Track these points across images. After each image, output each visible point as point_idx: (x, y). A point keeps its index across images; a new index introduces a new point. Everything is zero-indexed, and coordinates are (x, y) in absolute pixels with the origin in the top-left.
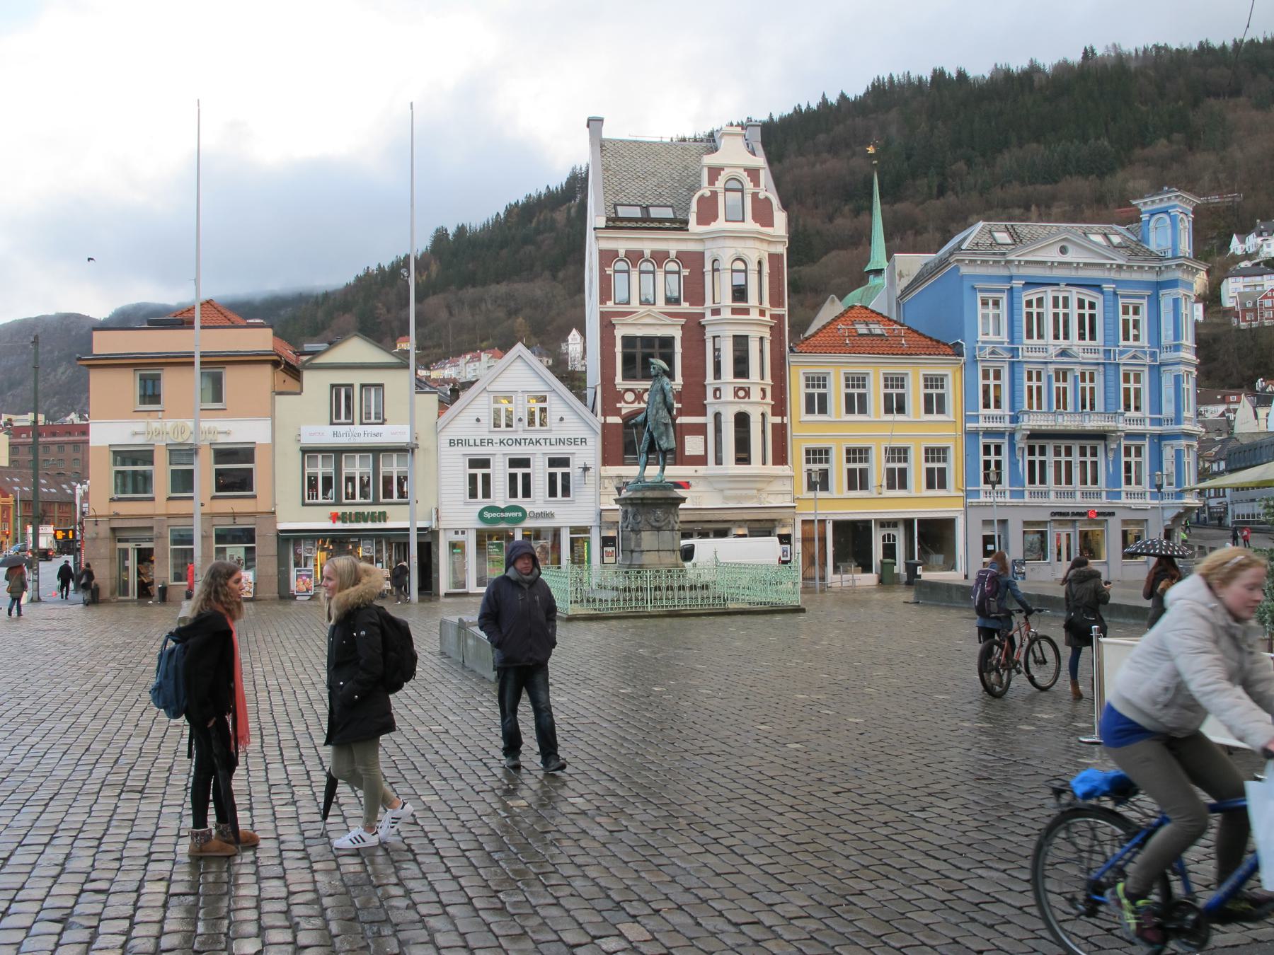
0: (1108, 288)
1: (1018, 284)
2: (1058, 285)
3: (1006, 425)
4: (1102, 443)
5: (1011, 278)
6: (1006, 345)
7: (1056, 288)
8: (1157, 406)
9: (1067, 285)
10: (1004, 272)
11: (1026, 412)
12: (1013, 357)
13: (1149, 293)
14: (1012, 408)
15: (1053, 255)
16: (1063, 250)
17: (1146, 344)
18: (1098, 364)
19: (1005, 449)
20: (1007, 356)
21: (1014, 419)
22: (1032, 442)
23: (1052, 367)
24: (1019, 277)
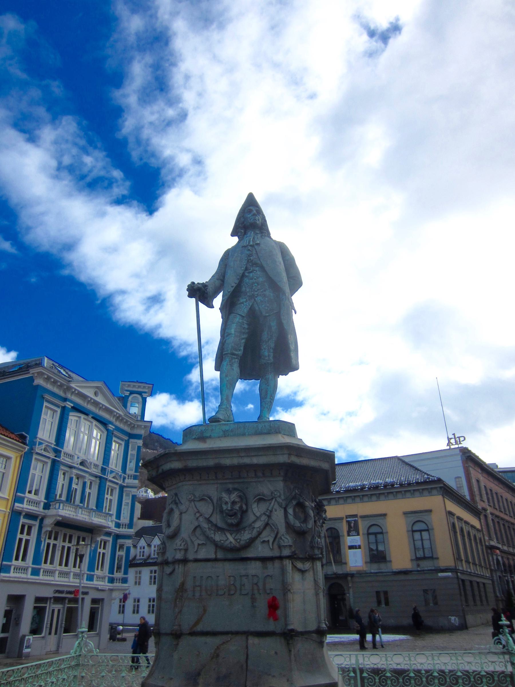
0: (111, 427)
1: (69, 405)
2: (87, 414)
3: (39, 510)
4: (90, 535)
5: (65, 400)
6: (53, 446)
7: (86, 417)
8: (118, 516)
9: (93, 418)
10: (61, 394)
11: (60, 502)
12: (55, 457)
13: (126, 438)
14: (47, 497)
15: (89, 393)
16: (96, 394)
17: (120, 470)
18: (96, 476)
19: (35, 531)
20: (52, 455)
21: (47, 506)
22: (58, 529)
23: (75, 471)
24: (71, 401)
